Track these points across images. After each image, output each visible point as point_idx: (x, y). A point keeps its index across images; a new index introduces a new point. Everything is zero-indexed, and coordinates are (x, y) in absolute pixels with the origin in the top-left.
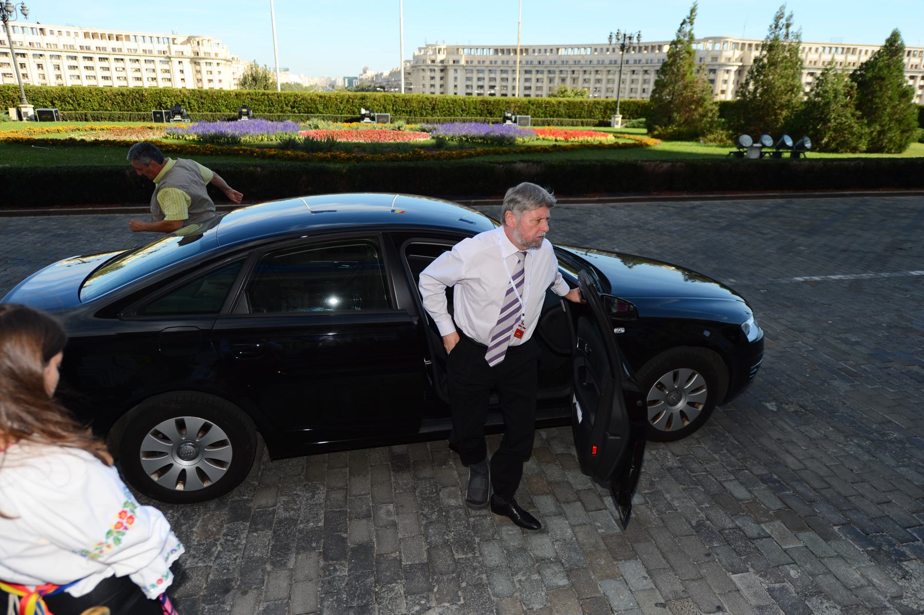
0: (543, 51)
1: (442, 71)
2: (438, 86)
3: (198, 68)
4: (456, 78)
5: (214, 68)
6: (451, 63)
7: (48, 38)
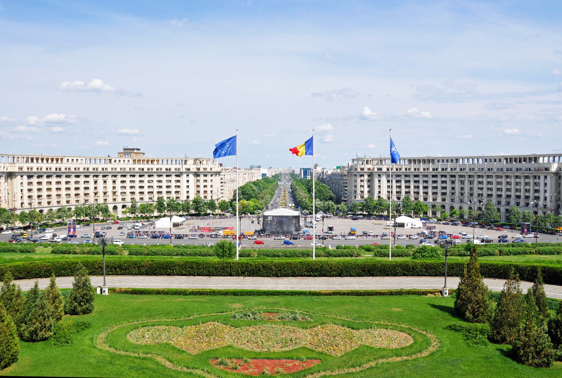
0: (445, 161)
3: (198, 178)
5: (209, 178)
6: (376, 170)
7: (113, 165)
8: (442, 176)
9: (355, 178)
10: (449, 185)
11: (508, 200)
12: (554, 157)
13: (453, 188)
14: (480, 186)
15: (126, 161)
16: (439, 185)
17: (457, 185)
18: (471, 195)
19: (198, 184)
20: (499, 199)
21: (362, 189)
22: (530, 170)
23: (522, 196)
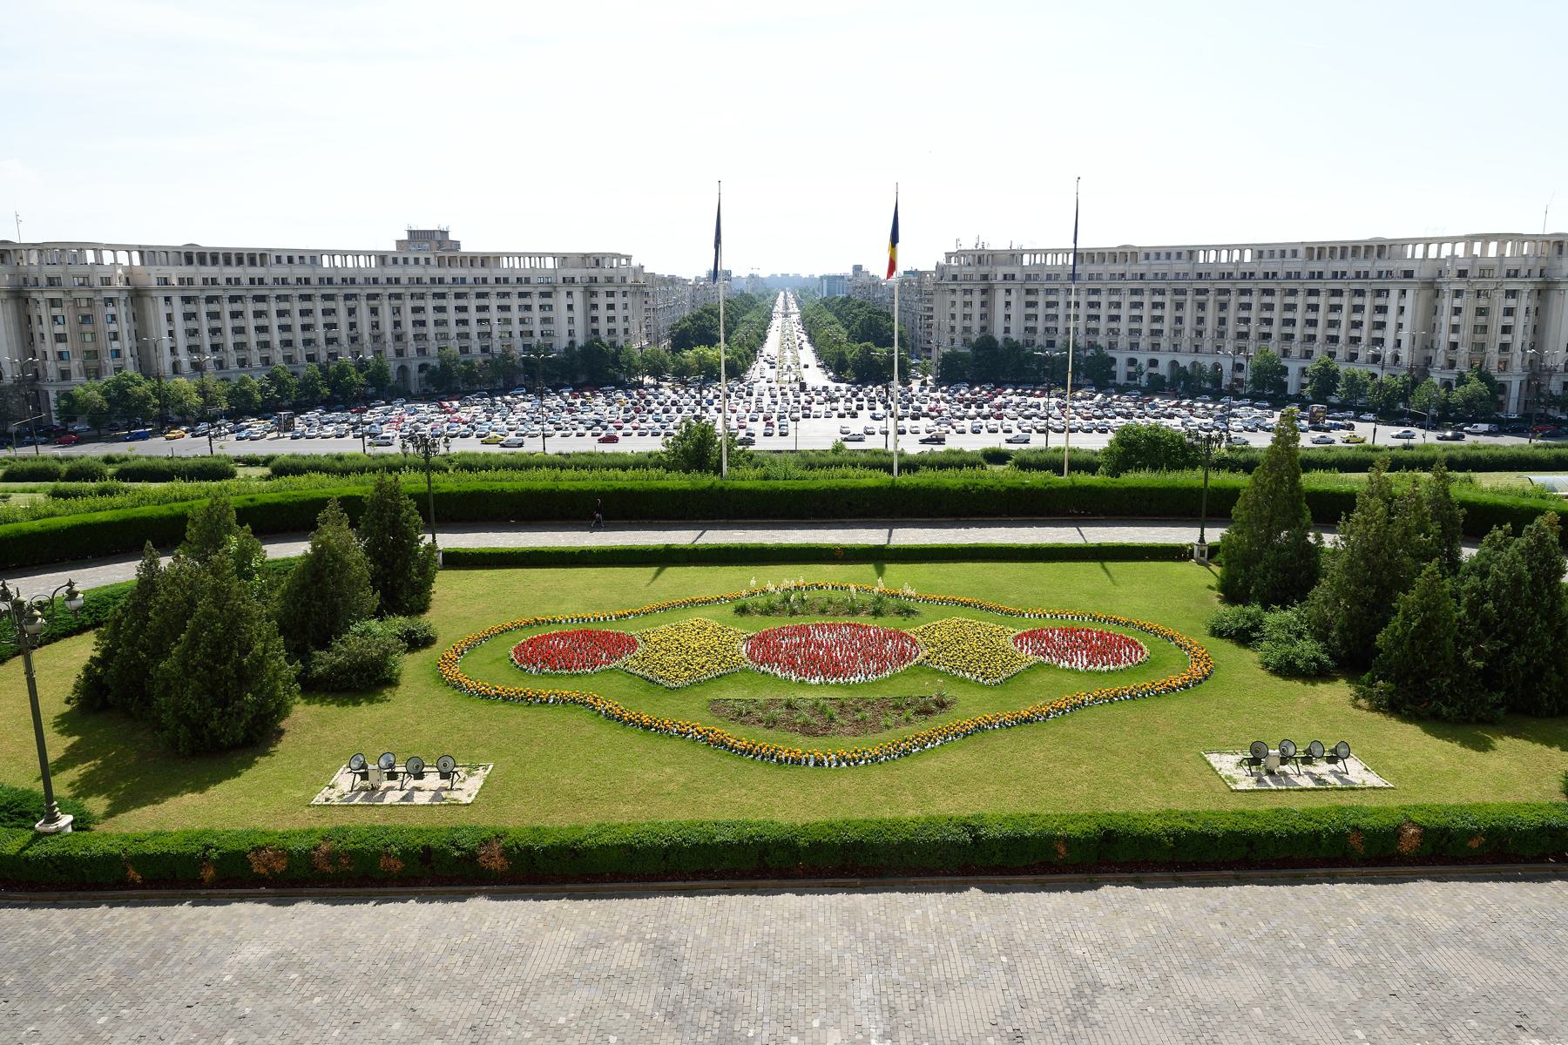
1: (984, 292)
2: (976, 317)
3: (594, 300)
4: (1008, 304)
5: (618, 300)
8: (1154, 291)
9: (953, 298)
10: (1168, 313)
11: (1308, 346)
12: (1427, 246)
13: (1179, 320)
14: (1244, 314)
15: (422, 261)
16: (1146, 312)
17: (1189, 314)
18: (1222, 335)
19: (594, 313)
20: (1286, 345)
21: (967, 323)
22: (1366, 274)
23: (1342, 338)
